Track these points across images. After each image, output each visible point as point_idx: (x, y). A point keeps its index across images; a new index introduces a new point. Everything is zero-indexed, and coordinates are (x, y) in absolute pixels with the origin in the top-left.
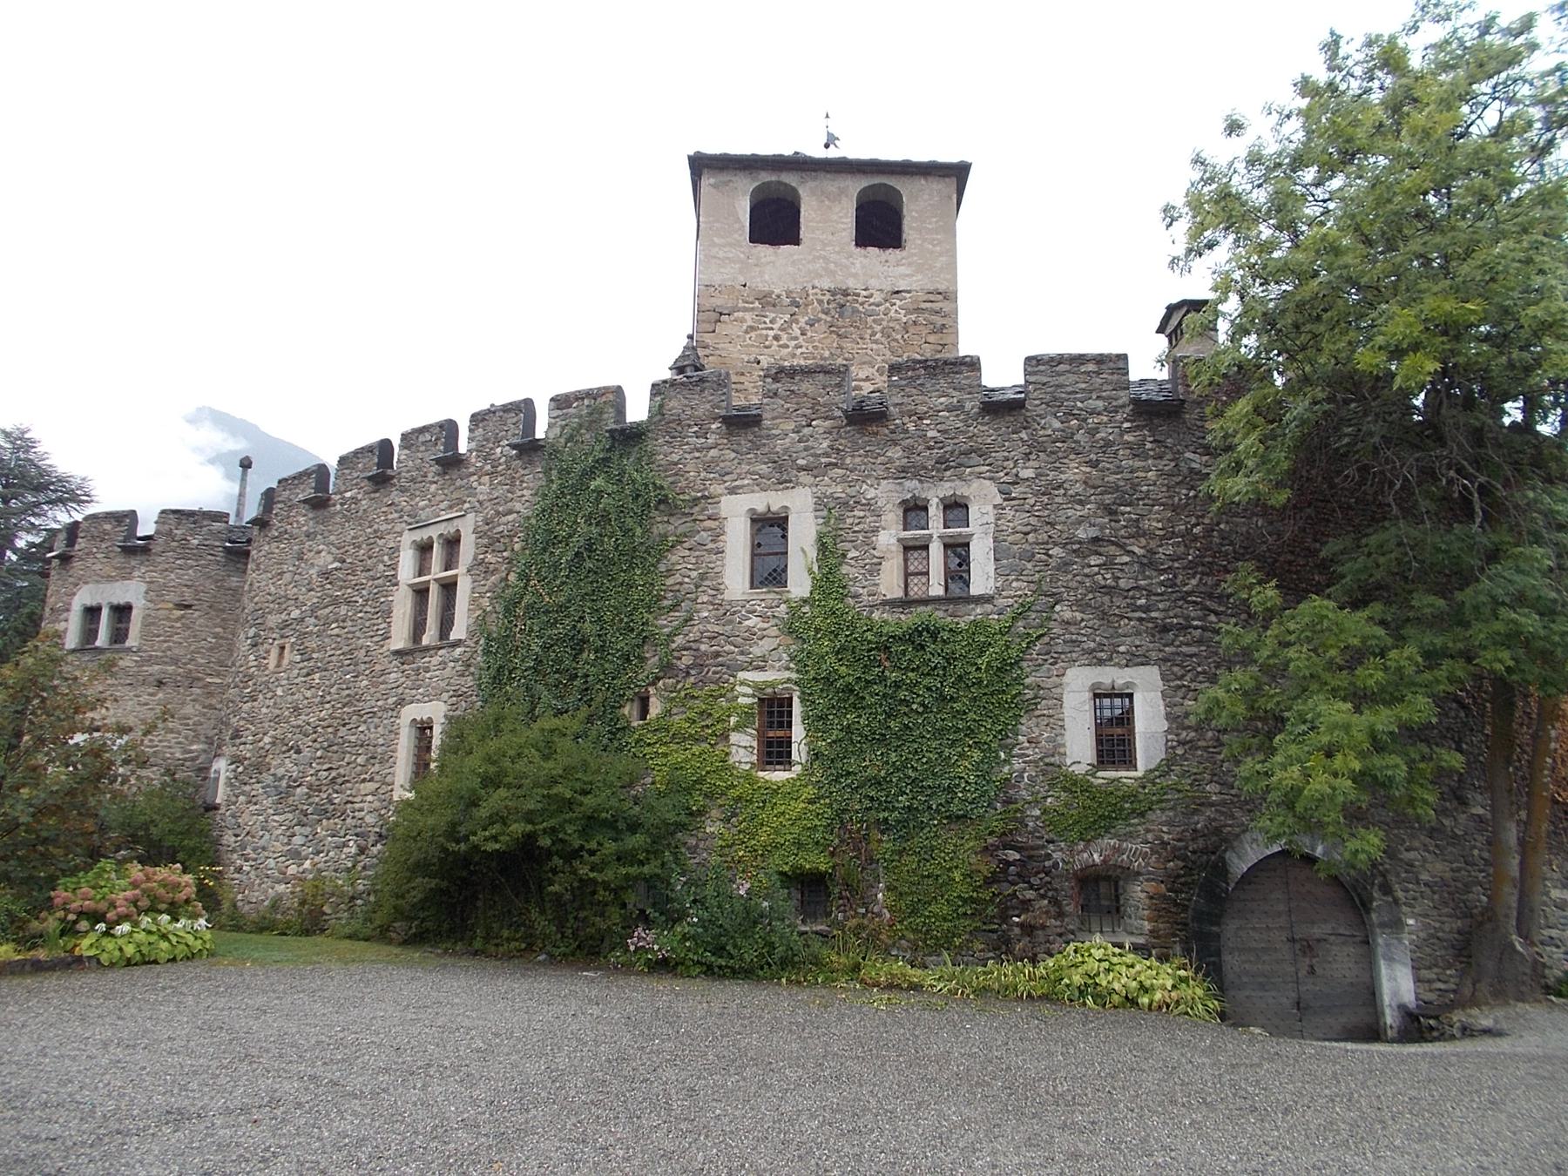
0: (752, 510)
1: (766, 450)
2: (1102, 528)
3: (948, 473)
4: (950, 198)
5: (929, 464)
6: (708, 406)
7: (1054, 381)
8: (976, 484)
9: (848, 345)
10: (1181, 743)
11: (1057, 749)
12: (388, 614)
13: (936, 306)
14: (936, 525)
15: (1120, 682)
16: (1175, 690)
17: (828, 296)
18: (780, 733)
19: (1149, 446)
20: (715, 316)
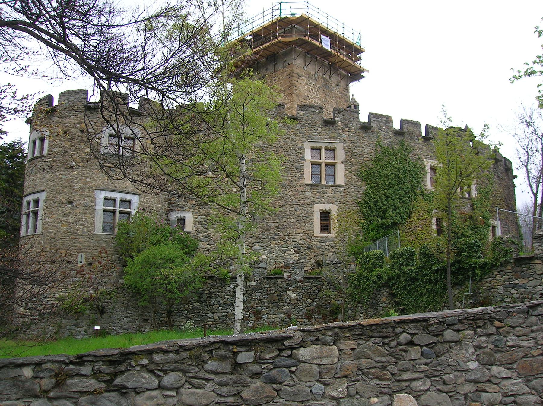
12: (300, 169)
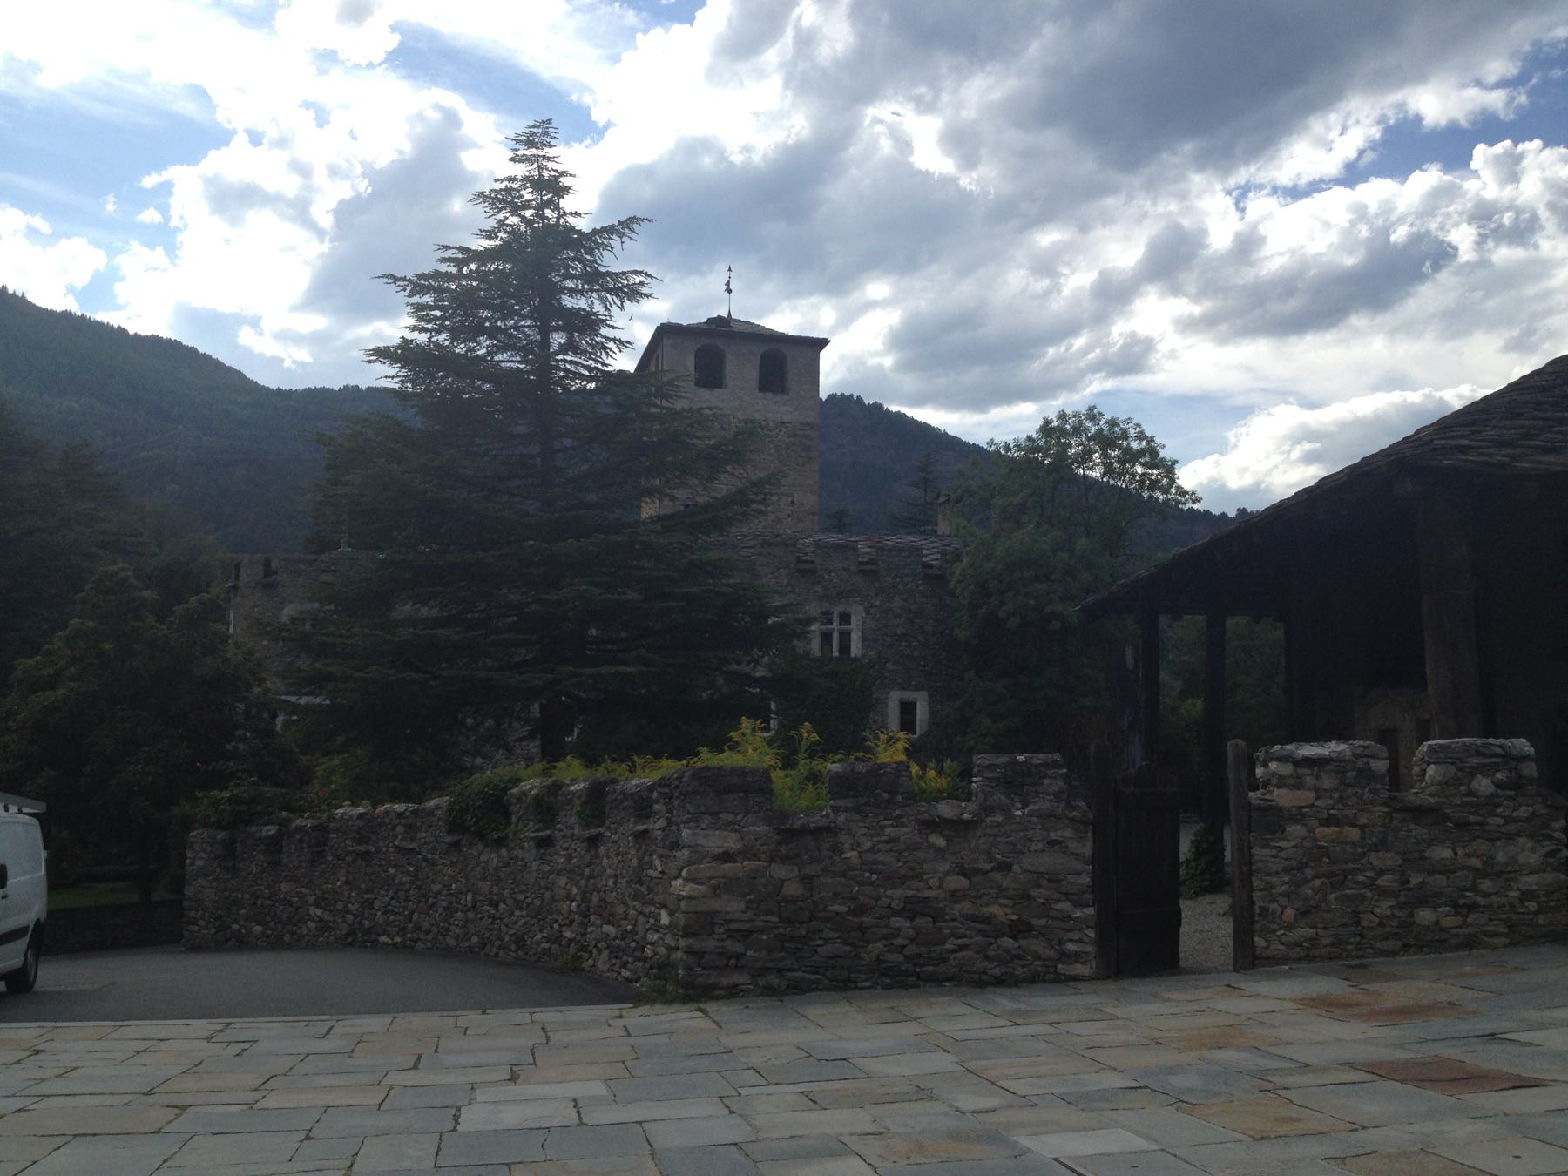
14: (836, 625)
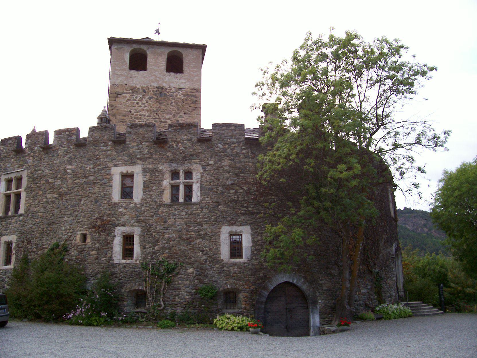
0: (122, 173)
1: (127, 152)
2: (234, 181)
3: (186, 162)
4: (199, 56)
5: (180, 158)
6: (108, 136)
7: (221, 132)
8: (195, 166)
9: (162, 107)
10: (256, 250)
11: (218, 252)
13: (194, 94)
15: (238, 231)
16: (257, 232)
17: (156, 89)
18: (130, 247)
19: (250, 154)
20: (115, 95)
